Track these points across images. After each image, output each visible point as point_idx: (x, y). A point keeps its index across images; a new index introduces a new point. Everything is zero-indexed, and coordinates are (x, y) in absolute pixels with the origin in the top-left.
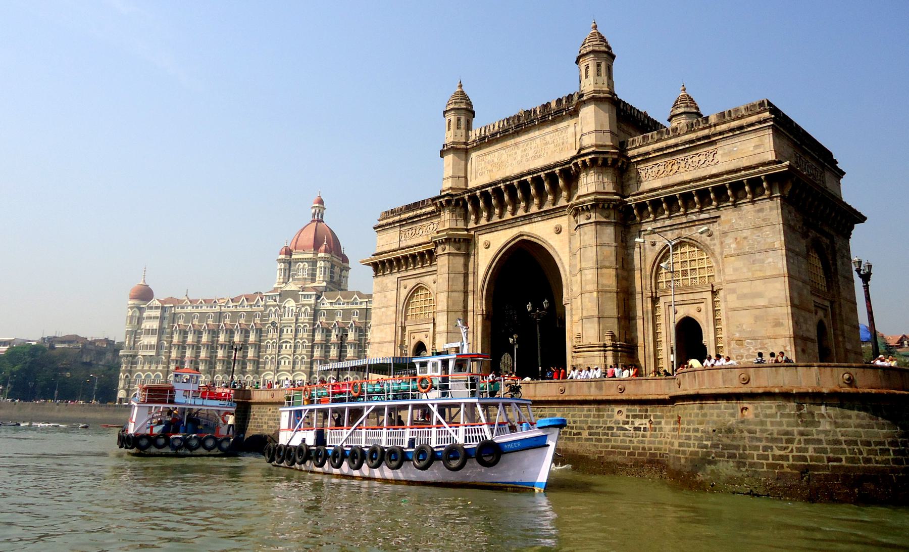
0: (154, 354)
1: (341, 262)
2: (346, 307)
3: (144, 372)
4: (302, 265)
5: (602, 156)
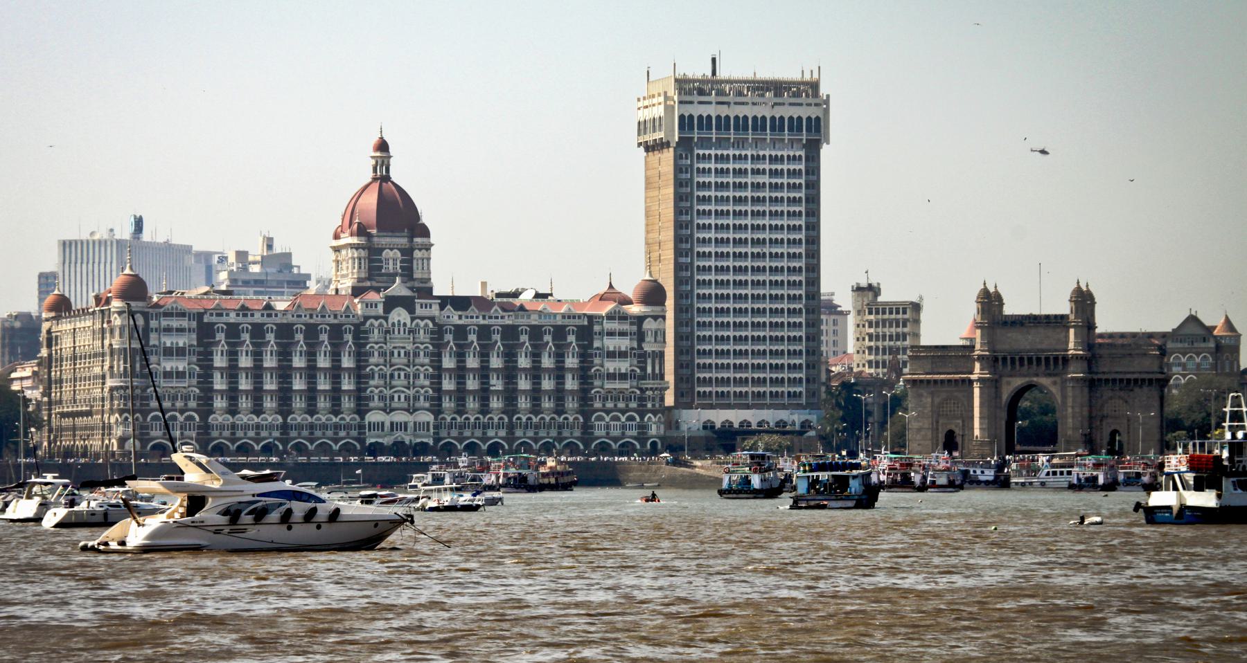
0: (186, 385)
2: (481, 321)
4: (391, 254)
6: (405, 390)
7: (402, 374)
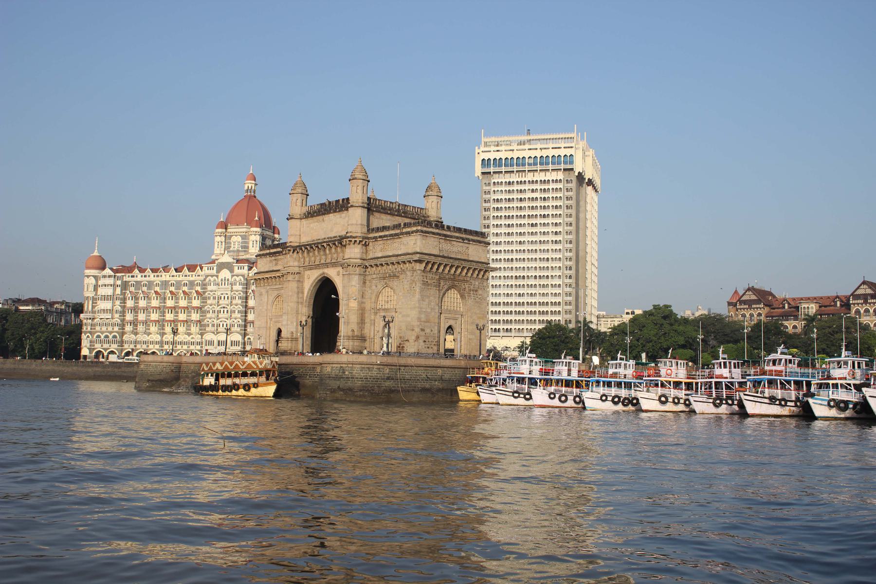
0: (110, 317)
1: (272, 234)
3: (102, 333)
5: (353, 240)
6: (226, 320)
7: (226, 310)
